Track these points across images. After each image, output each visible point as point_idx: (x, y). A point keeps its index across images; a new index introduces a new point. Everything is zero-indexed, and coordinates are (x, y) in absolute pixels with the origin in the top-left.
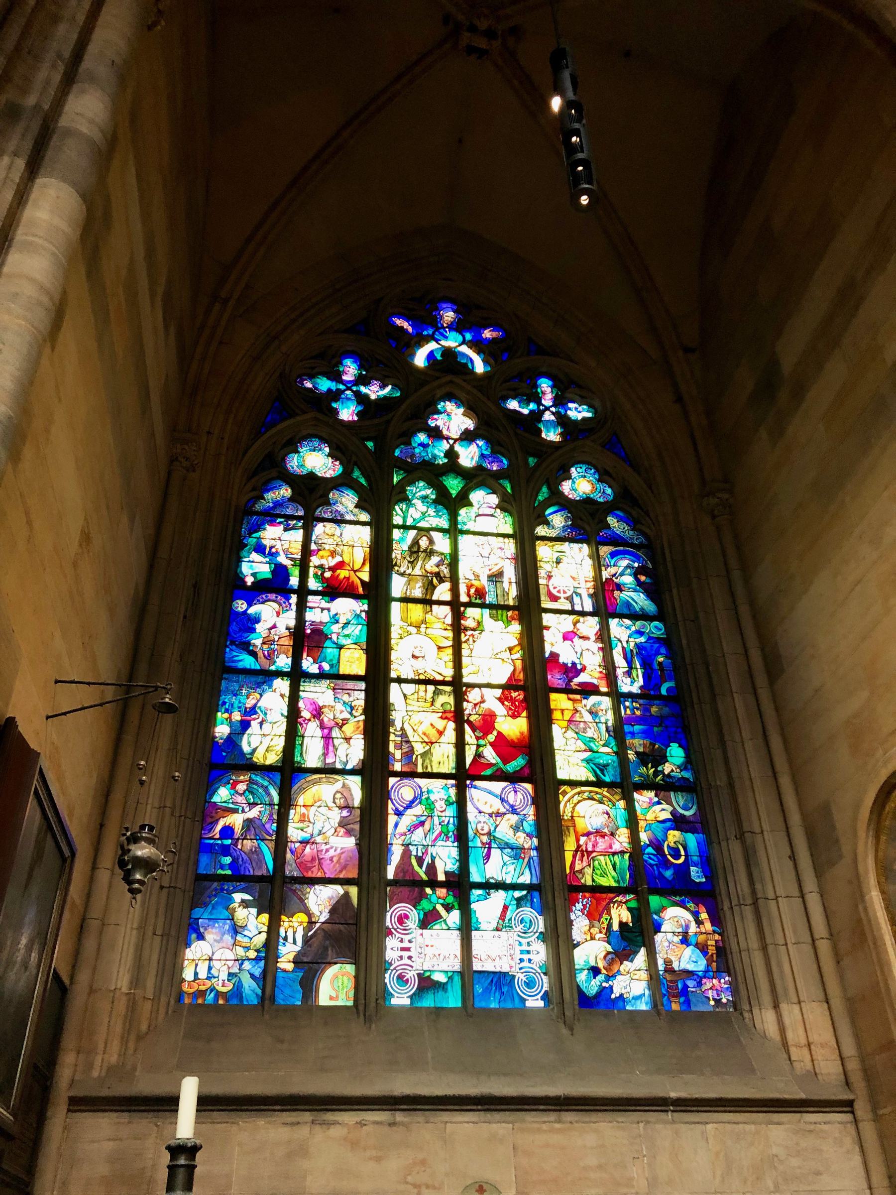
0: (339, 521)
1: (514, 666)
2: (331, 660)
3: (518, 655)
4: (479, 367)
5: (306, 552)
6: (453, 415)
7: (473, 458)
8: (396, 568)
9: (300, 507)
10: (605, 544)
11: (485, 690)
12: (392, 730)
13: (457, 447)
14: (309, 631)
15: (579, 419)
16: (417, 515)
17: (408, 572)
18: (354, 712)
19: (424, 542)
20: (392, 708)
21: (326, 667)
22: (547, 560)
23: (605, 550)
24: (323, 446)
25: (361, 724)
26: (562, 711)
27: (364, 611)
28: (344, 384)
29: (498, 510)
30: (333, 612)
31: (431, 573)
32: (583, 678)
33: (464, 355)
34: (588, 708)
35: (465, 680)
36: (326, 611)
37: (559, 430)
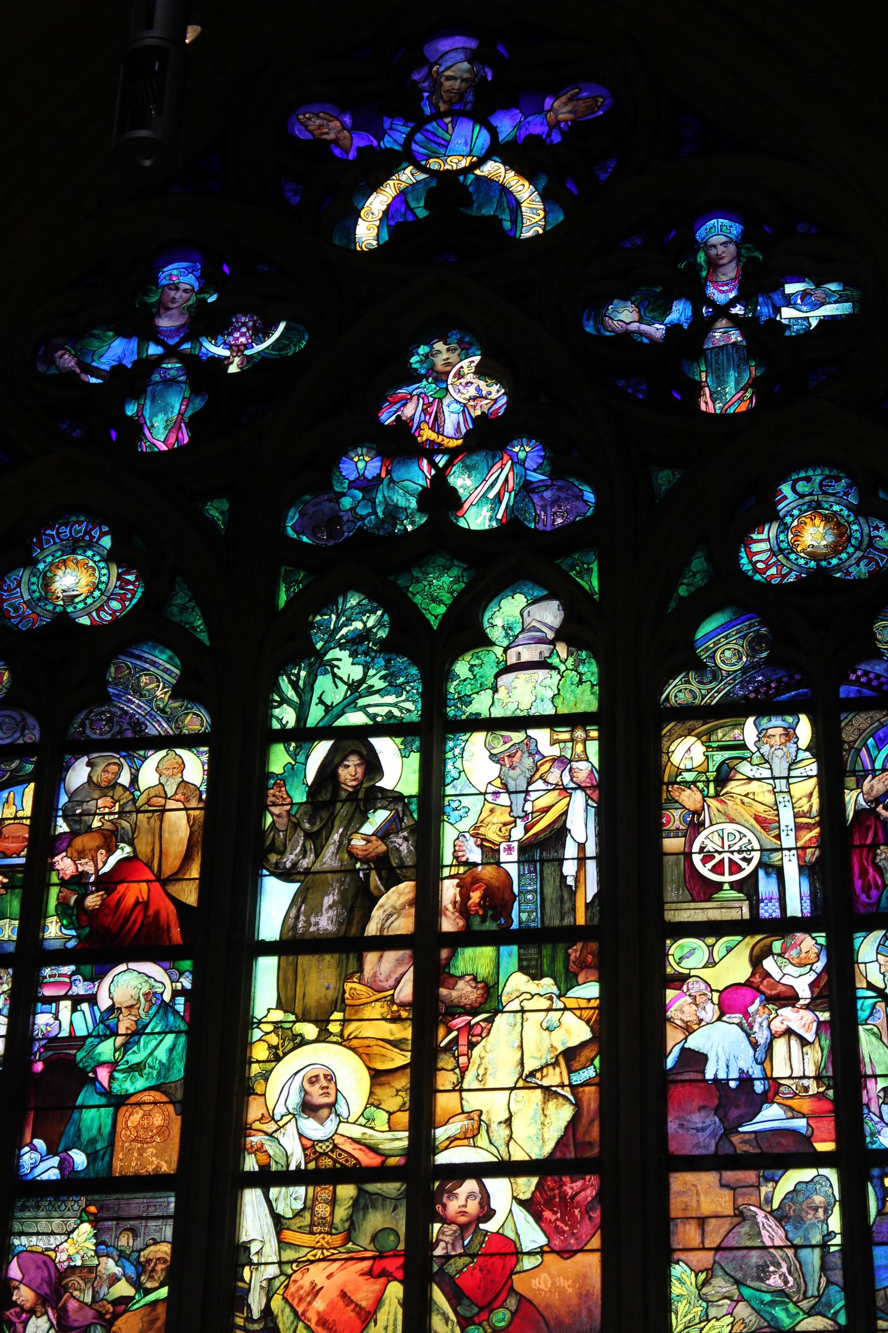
0: (134, 743)
1: (578, 1105)
2: (93, 1141)
3: (590, 1073)
4: (533, 216)
5: (42, 842)
6: (450, 379)
7: (499, 498)
8: (273, 858)
9: (31, 721)
10: (858, 705)
11: (488, 1182)
12: (240, 1321)
13: (460, 481)
14: (39, 1067)
15: (814, 323)
16: (336, 695)
17: (305, 863)
18: (143, 1278)
19: (350, 772)
20: (243, 1259)
21: (79, 1159)
22: (689, 777)
23: (854, 725)
24: (96, 533)
25: (161, 1310)
26: (702, 1221)
27: (183, 992)
28: (159, 342)
29: (562, 649)
30: (104, 1003)
31: (365, 860)
32: (771, 1116)
33: (486, 182)
34: (775, 1205)
35: (441, 1159)
36: (85, 1006)
37: (752, 371)
